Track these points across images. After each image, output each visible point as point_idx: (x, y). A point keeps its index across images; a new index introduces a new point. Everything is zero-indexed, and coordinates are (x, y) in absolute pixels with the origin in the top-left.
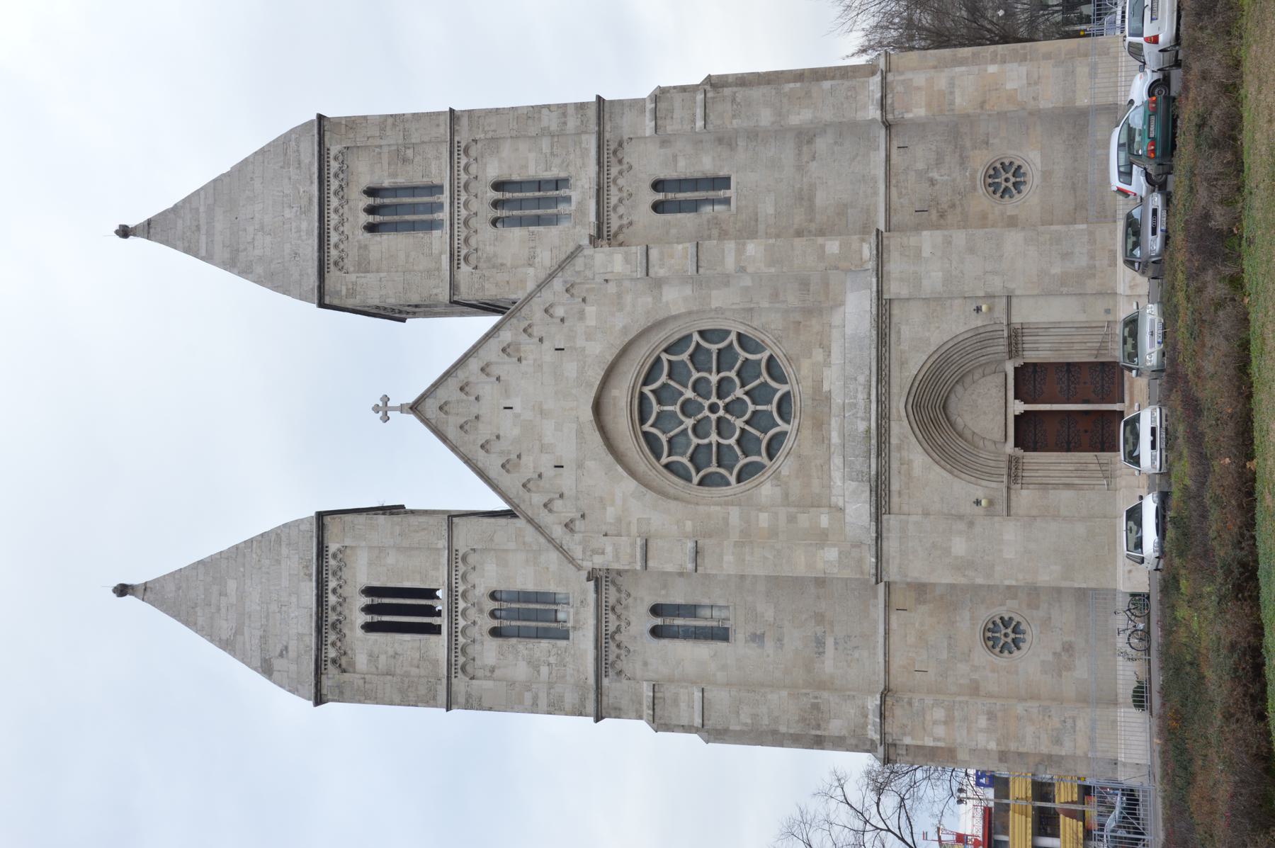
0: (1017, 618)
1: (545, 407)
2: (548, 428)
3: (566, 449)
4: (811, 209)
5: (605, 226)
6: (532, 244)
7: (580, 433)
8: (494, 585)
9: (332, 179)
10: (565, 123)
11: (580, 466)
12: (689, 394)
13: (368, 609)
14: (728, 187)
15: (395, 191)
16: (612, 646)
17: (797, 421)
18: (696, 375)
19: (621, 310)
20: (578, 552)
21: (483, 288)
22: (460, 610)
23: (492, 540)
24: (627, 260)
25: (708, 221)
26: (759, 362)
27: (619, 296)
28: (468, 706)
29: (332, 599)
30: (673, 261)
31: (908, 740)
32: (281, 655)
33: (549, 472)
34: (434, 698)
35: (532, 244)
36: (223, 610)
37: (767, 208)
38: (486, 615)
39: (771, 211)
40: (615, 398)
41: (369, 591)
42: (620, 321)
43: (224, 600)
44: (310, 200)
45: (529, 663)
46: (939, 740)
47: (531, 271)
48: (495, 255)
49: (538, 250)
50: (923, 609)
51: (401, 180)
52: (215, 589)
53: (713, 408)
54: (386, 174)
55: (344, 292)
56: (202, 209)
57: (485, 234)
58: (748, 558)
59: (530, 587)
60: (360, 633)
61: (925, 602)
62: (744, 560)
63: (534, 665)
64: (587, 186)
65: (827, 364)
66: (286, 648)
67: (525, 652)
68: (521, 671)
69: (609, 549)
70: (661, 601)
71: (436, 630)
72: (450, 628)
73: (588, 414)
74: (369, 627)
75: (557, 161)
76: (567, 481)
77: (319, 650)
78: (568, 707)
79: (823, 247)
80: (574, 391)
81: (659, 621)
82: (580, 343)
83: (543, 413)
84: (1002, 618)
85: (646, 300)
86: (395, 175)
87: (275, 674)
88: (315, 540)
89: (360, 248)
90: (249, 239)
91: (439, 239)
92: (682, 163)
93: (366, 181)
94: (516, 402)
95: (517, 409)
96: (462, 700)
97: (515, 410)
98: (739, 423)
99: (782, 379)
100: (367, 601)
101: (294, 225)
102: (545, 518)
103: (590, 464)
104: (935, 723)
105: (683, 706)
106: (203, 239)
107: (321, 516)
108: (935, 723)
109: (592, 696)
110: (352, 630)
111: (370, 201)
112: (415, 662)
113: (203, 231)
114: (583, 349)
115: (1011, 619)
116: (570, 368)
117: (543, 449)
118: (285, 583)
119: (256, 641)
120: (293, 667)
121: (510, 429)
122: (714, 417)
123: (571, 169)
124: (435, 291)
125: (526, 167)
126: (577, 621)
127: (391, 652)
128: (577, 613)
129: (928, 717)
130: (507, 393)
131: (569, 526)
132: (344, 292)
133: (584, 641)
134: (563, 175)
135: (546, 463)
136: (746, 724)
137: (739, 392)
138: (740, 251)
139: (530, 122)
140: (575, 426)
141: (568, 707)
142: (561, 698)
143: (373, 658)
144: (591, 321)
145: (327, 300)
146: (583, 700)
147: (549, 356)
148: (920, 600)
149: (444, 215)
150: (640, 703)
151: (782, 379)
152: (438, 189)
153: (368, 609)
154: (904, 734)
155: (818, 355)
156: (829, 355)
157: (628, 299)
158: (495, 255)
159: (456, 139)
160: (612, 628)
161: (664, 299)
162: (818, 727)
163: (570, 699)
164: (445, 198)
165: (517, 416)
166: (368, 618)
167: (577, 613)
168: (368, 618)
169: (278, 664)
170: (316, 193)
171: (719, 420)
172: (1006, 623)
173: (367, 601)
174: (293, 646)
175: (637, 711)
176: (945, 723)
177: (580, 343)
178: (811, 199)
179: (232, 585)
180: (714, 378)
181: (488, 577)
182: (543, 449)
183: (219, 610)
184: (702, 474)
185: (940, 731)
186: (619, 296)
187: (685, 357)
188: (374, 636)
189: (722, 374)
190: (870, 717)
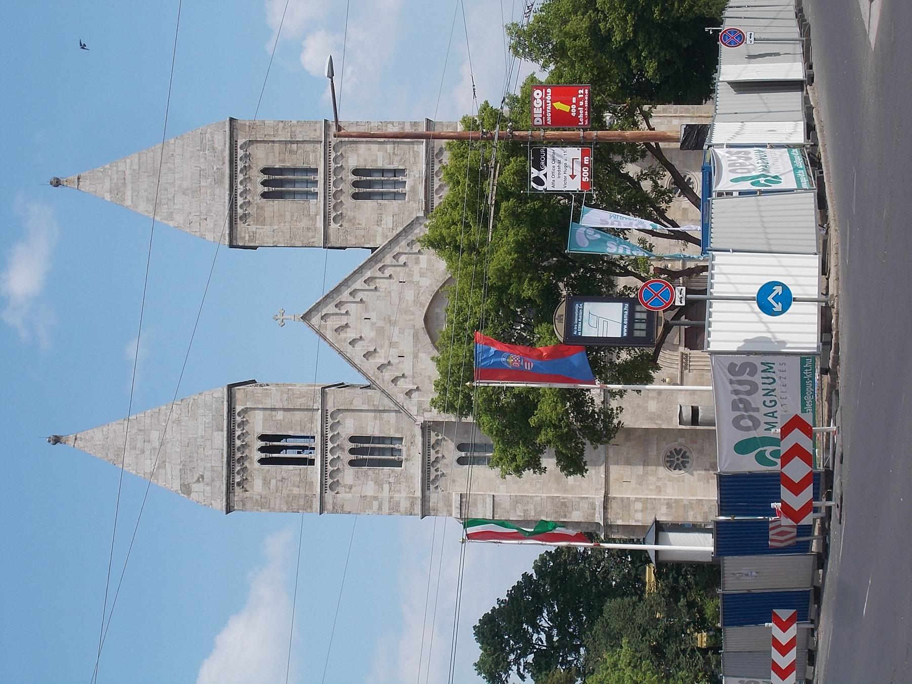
0: (684, 449)
3: (406, 345)
6: (379, 212)
7: (415, 336)
8: (352, 433)
9: (239, 162)
11: (416, 356)
13: (262, 450)
15: (281, 171)
16: (432, 470)
20: (414, 411)
22: (329, 449)
23: (351, 403)
28: (334, 511)
31: (619, 522)
32: (198, 481)
33: (395, 361)
34: (311, 507)
35: (379, 212)
36: (147, 452)
38: (347, 452)
40: (437, 314)
41: (263, 438)
43: (148, 446)
44: (223, 174)
45: (376, 482)
46: (638, 521)
47: (380, 229)
48: (354, 218)
49: (384, 216)
50: (628, 444)
51: (288, 164)
52: (140, 437)
54: (277, 160)
55: (247, 238)
56: (128, 172)
59: (377, 434)
60: (257, 465)
61: (630, 440)
63: (379, 484)
64: (417, 176)
66: (202, 477)
67: (373, 476)
68: (370, 489)
70: (464, 442)
71: (312, 462)
72: (322, 461)
73: (421, 323)
74: (262, 461)
75: (397, 158)
77: (228, 477)
78: (402, 509)
81: (463, 454)
82: (416, 278)
84: (675, 449)
86: (284, 161)
87: (193, 495)
88: (225, 403)
89: (258, 208)
90: (170, 196)
91: (316, 205)
93: (263, 164)
94: (373, 315)
95: (374, 320)
96: (329, 506)
97: (372, 320)
100: (263, 444)
101: (209, 191)
102: (391, 389)
103: (422, 355)
104: (636, 511)
105: (480, 506)
106: (129, 194)
107: (230, 387)
108: (636, 511)
109: (419, 502)
110: (251, 463)
111: (266, 177)
112: (297, 483)
113: (129, 186)
115: (681, 450)
116: (409, 295)
117: (391, 344)
118: (201, 432)
119: (177, 473)
120: (208, 489)
121: (368, 332)
123: (407, 164)
124: (312, 240)
126: (409, 455)
127: (279, 478)
128: (409, 449)
129: (632, 508)
130: (366, 309)
131: (409, 393)
132: (247, 238)
133: (414, 467)
134: (401, 167)
136: (520, 516)
142: (398, 503)
143: (266, 482)
145: (234, 244)
146: (412, 504)
148: (627, 439)
149: (320, 189)
150: (451, 506)
152: (315, 171)
153: (262, 450)
154: (617, 519)
158: (354, 218)
159: (328, 140)
160: (432, 459)
162: (565, 516)
163: (404, 505)
164: (320, 177)
166: (263, 455)
167: (409, 449)
168: (263, 455)
169: (195, 487)
170: (227, 171)
172: (678, 452)
173: (263, 444)
174: (208, 475)
175: (448, 511)
176: (642, 511)
177: (416, 278)
179: (155, 435)
181: (349, 427)
182: (391, 344)
183: (143, 452)
185: (639, 516)
188: (266, 467)
190: (597, 509)
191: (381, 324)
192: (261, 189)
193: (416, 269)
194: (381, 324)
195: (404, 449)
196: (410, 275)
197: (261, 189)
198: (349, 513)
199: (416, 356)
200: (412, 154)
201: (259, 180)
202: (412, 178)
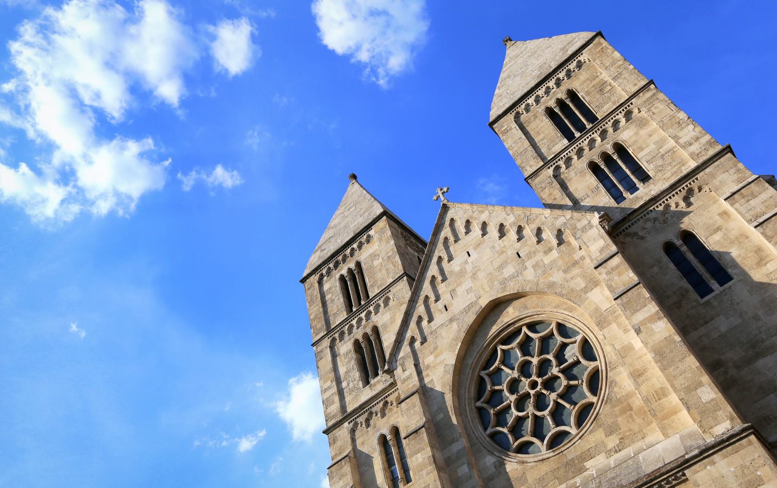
1: (478, 273)
2: (467, 284)
3: (459, 304)
4: (749, 361)
5: (630, 223)
6: (590, 193)
10: (691, 144)
11: (451, 320)
12: (535, 361)
14: (721, 284)
17: (552, 454)
18: (550, 357)
19: (565, 272)
21: (543, 189)
24: (601, 251)
25: (680, 288)
26: (585, 397)
27: (575, 263)
29: (348, 251)
30: (616, 278)
33: (440, 305)
37: (723, 324)
39: (723, 329)
42: (557, 277)
53: (534, 385)
57: (580, 164)
58: (424, 472)
60: (338, 276)
62: (422, 470)
65: (609, 453)
69: (407, 373)
73: (484, 302)
76: (440, 318)
79: (700, 384)
80: (496, 283)
82: (529, 264)
83: (474, 276)
85: (581, 283)
92: (717, 237)
95: (470, 260)
98: (530, 409)
99: (579, 423)
103: (455, 325)
114: (526, 268)
116: (509, 270)
122: (527, 389)
125: (641, 149)
135: (445, 298)
137: (553, 396)
138: (651, 319)
139: (676, 126)
140: (474, 299)
141: (329, 410)
144: (547, 260)
147: (511, 253)
151: (579, 423)
155: (612, 442)
156: (616, 452)
157: (576, 271)
161: (588, 295)
165: (466, 262)
171: (527, 395)
178: (759, 355)
180: (555, 371)
184: (485, 405)
186: (575, 263)
187: (559, 339)
189: (560, 375)
191: (469, 268)
192: (552, 103)
193: (539, 256)
194: (469, 268)
195: (379, 378)
196: (530, 255)
197: (552, 103)
198: (318, 367)
199: (451, 320)
200: (675, 169)
201: (559, 96)
202: (646, 190)
